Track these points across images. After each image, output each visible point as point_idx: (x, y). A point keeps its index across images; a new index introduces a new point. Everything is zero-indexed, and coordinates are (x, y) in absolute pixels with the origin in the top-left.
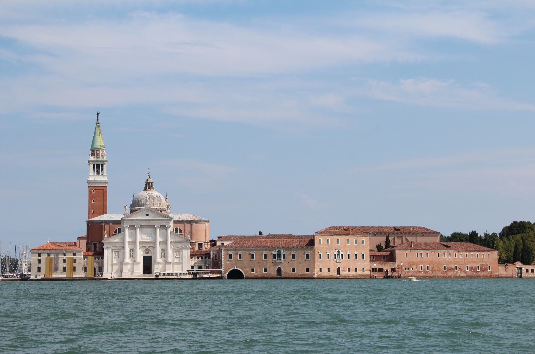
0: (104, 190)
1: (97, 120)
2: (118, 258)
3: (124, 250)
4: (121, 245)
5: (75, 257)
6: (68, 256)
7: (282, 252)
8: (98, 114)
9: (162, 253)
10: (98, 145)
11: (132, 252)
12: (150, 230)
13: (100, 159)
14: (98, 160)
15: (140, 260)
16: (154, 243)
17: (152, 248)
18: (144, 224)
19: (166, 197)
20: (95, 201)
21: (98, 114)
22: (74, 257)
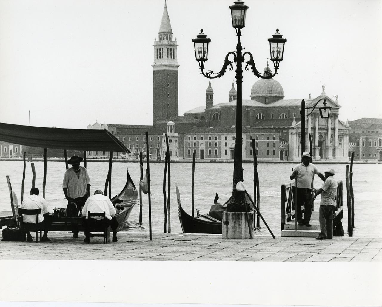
1: (166, 4)
13: (172, 43)
16: (327, 130)
22: (274, 141)
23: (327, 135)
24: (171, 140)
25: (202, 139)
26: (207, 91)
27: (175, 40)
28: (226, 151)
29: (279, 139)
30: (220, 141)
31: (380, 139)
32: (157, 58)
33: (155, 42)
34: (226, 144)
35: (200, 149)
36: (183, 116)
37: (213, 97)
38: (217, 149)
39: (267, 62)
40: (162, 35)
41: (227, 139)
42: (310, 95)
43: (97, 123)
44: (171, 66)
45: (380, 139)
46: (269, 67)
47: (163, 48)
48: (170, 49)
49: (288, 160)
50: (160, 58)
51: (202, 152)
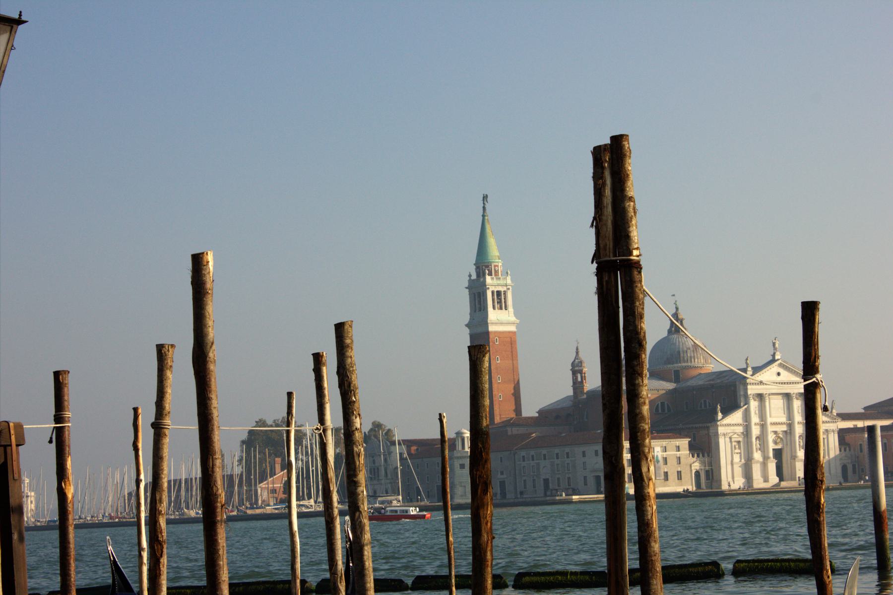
0: (513, 339)
1: (484, 208)
2: (740, 453)
3: (747, 438)
5: (680, 452)
6: (669, 451)
8: (485, 198)
9: (799, 442)
10: (495, 256)
11: (758, 442)
13: (501, 282)
14: (499, 282)
15: (771, 454)
20: (501, 360)
21: (485, 198)
22: (678, 453)
23: (790, 433)
25: (545, 459)
26: (573, 364)
28: (585, 478)
29: (687, 446)
32: (475, 311)
33: (471, 281)
35: (543, 477)
36: (537, 415)
37: (585, 376)
38: (570, 475)
44: (502, 324)
46: (680, 311)
49: (712, 489)
50: (480, 311)
51: (546, 481)
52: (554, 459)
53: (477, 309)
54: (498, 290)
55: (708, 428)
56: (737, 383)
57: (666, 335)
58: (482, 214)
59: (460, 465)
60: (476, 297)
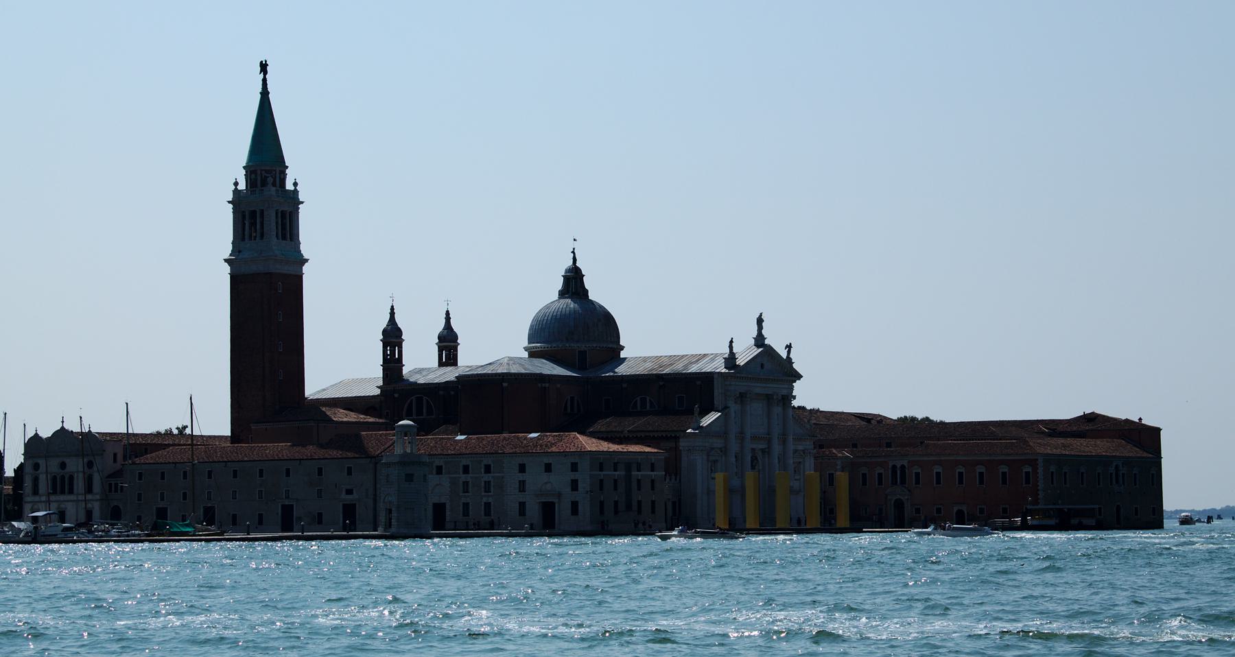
1: (264, 81)
4: (718, 443)
5: (655, 473)
7: (1121, 468)
12: (757, 408)
17: (760, 453)
18: (758, 388)
19: (448, 313)
21: (264, 67)
24: (412, 475)
26: (385, 332)
27: (293, 188)
28: (522, 505)
30: (503, 477)
31: (894, 467)
32: (243, 239)
33: (236, 192)
34: (522, 486)
38: (490, 500)
39: (573, 252)
40: (259, 172)
41: (525, 472)
42: (731, 342)
43: (63, 428)
45: (894, 467)
47: (262, 212)
48: (282, 211)
52: (459, 474)
53: (247, 237)
54: (282, 209)
55: (676, 439)
56: (716, 376)
57: (556, 296)
58: (260, 89)
59: (407, 475)
60: (247, 217)
